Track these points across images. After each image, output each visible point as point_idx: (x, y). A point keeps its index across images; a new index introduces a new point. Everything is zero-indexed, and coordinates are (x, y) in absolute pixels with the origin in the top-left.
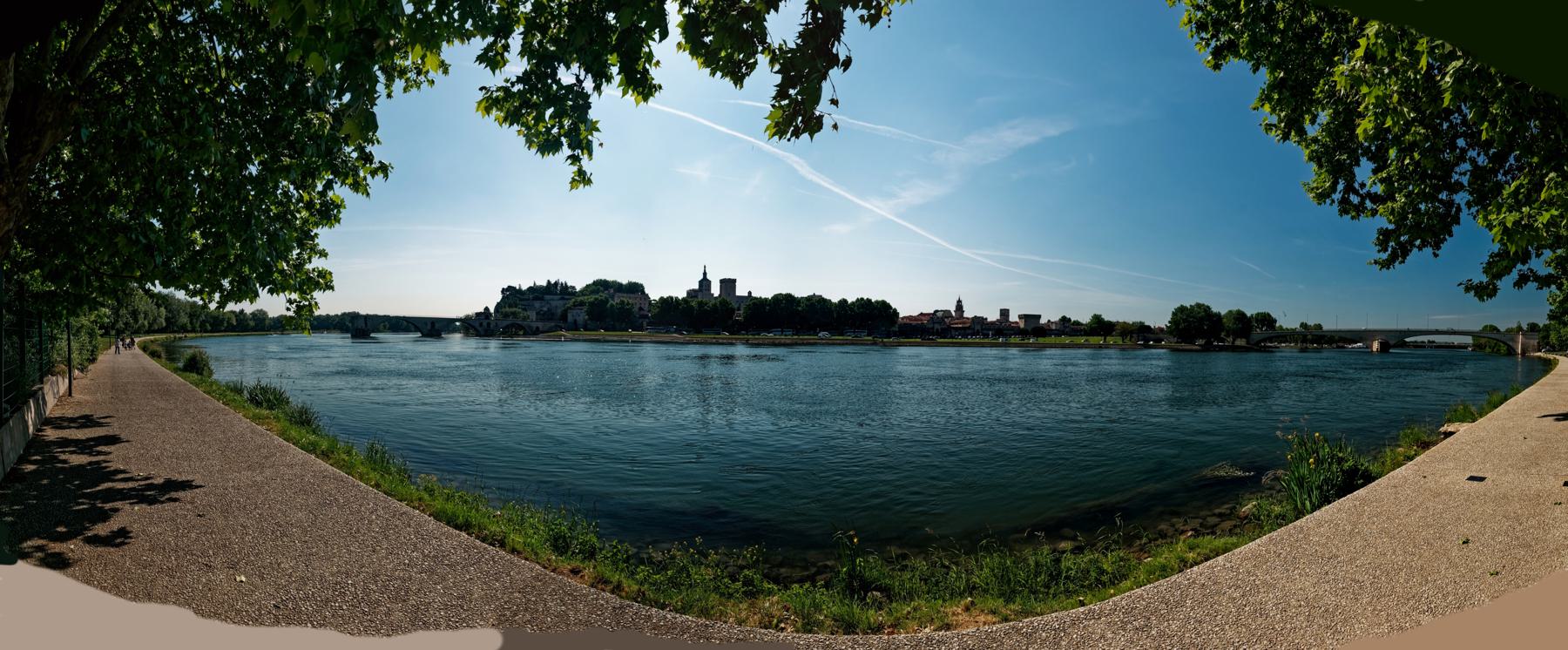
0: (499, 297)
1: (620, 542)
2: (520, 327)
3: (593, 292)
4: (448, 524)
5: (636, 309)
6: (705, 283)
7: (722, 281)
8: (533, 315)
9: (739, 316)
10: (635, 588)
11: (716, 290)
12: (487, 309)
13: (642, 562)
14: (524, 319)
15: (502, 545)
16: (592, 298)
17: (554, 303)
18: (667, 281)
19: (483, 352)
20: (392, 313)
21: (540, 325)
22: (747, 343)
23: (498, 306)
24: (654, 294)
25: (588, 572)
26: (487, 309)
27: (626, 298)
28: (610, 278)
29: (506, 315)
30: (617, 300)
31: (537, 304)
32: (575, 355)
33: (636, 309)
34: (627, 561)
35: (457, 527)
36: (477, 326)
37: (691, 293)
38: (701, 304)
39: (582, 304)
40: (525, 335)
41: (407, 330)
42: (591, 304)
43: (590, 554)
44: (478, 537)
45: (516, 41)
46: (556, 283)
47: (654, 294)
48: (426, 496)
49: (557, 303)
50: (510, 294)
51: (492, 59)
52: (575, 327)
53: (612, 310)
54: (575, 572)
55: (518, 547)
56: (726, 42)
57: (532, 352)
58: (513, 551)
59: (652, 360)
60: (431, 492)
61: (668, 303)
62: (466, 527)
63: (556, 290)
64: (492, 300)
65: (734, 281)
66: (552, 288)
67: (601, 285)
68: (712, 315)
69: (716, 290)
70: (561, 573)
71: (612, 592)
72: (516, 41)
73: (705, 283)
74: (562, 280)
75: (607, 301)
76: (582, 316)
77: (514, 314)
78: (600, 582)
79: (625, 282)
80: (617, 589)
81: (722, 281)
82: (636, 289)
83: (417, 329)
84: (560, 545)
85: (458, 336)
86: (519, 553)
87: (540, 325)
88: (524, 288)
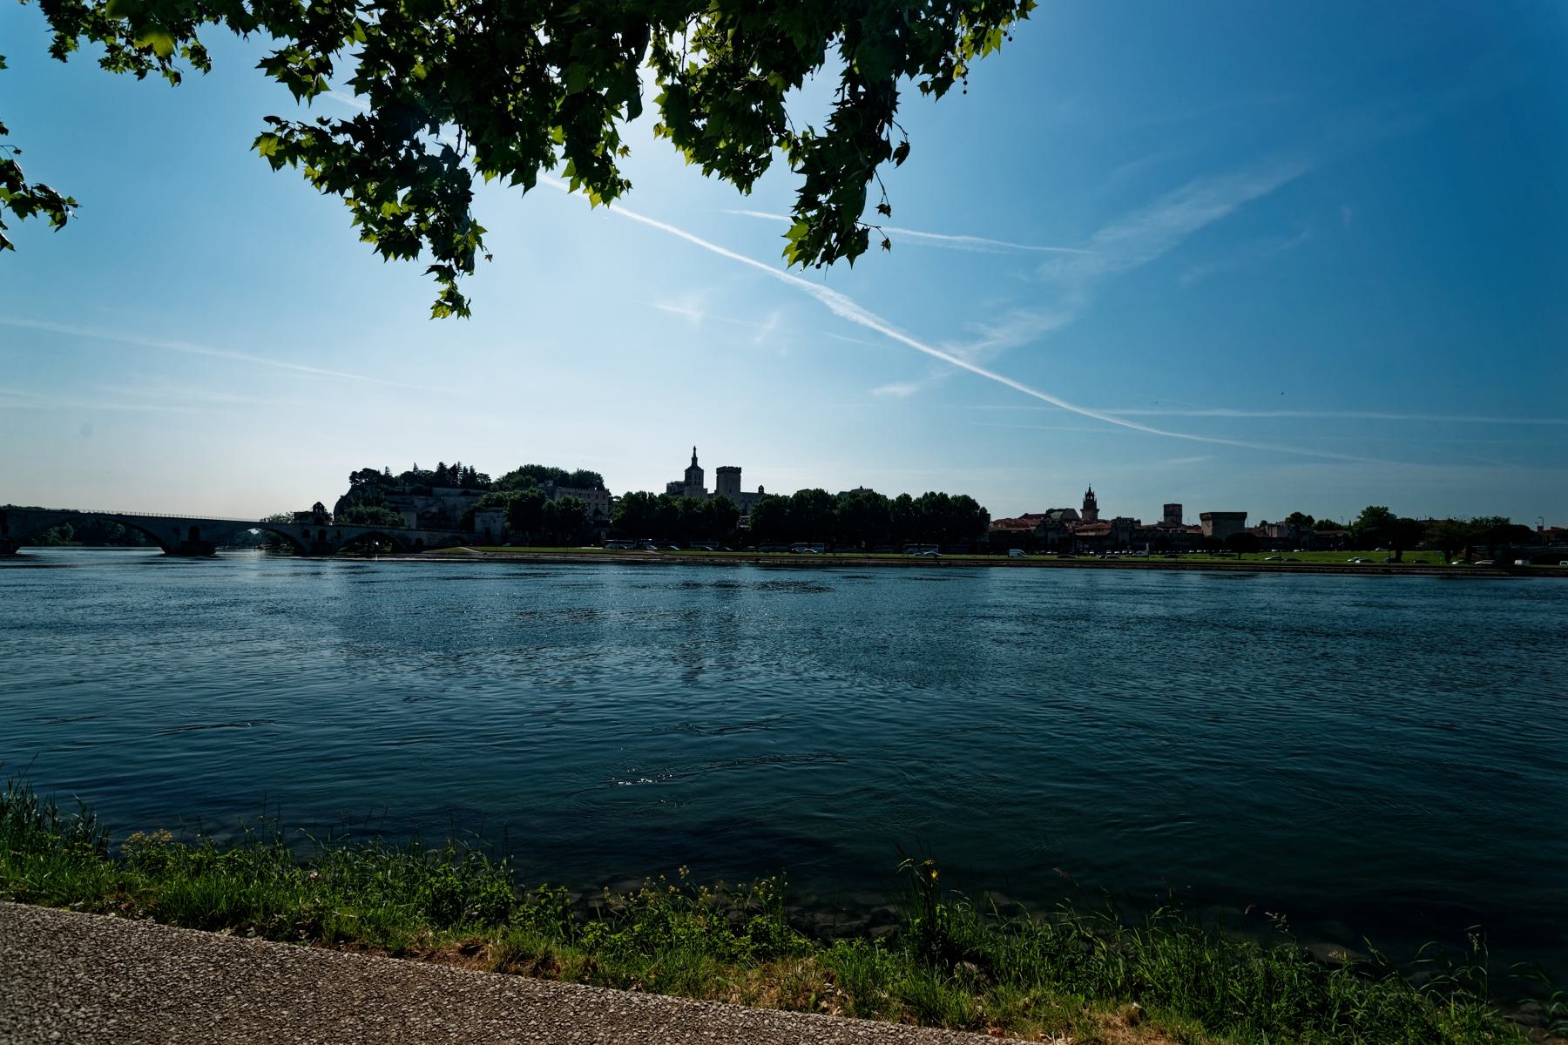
0: (345, 487)
1: (552, 886)
2: (384, 539)
3: (518, 485)
4: (190, 921)
5: (589, 513)
6: (694, 473)
7: (721, 471)
8: (411, 519)
9: (746, 523)
10: (582, 958)
11: (710, 484)
12: (319, 506)
13: (592, 914)
14: (395, 525)
15: (315, 932)
16: (516, 494)
17: (451, 501)
18: (638, 470)
19: (304, 582)
20: (85, 506)
21: (424, 535)
22: (756, 563)
23: (343, 503)
24: (617, 487)
25: (494, 945)
26: (319, 506)
27: (572, 495)
28: (548, 464)
29: (358, 519)
30: (558, 499)
31: (419, 502)
32: (490, 588)
33: (589, 513)
34: (563, 915)
35: (214, 925)
36: (300, 536)
37: (673, 488)
38: (688, 504)
39: (500, 502)
40: (394, 552)
41: (126, 541)
42: (516, 504)
43: (498, 914)
44: (260, 931)
45: (347, 59)
46: (455, 469)
47: (617, 487)
48: (140, 878)
49: (454, 499)
50: (368, 484)
51: (304, 84)
52: (486, 539)
53: (550, 515)
54: (468, 951)
55: (348, 929)
56: (724, 127)
57: (401, 582)
58: (340, 939)
59: (612, 586)
60: (155, 868)
61: (637, 502)
62: (237, 918)
63: (453, 482)
64: (330, 491)
65: (739, 470)
66: (446, 475)
67: (532, 475)
68: (705, 521)
69: (710, 484)
70: (445, 959)
71: (534, 973)
72: (347, 59)
73: (694, 473)
74: (466, 464)
75: (541, 499)
76: (499, 522)
77: (375, 517)
78: (513, 960)
79: (571, 470)
80: (544, 968)
81: (721, 471)
82: (589, 482)
83: (152, 541)
84: (445, 911)
85: (254, 555)
86: (348, 939)
87: (424, 535)
88: (396, 473)
